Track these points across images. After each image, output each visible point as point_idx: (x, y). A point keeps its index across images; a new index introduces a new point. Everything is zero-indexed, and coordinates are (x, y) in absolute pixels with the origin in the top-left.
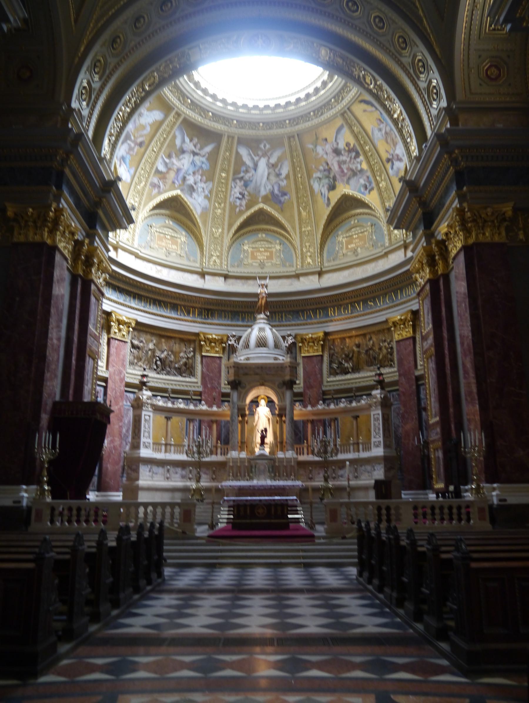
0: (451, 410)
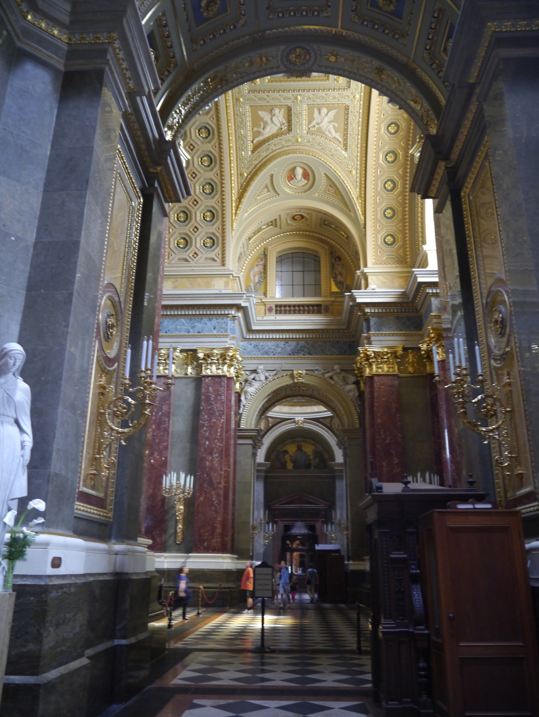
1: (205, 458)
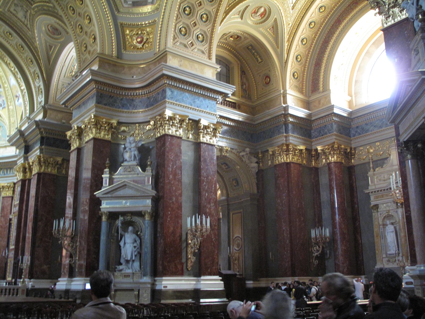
0: (20, 244)
1: (206, 206)
